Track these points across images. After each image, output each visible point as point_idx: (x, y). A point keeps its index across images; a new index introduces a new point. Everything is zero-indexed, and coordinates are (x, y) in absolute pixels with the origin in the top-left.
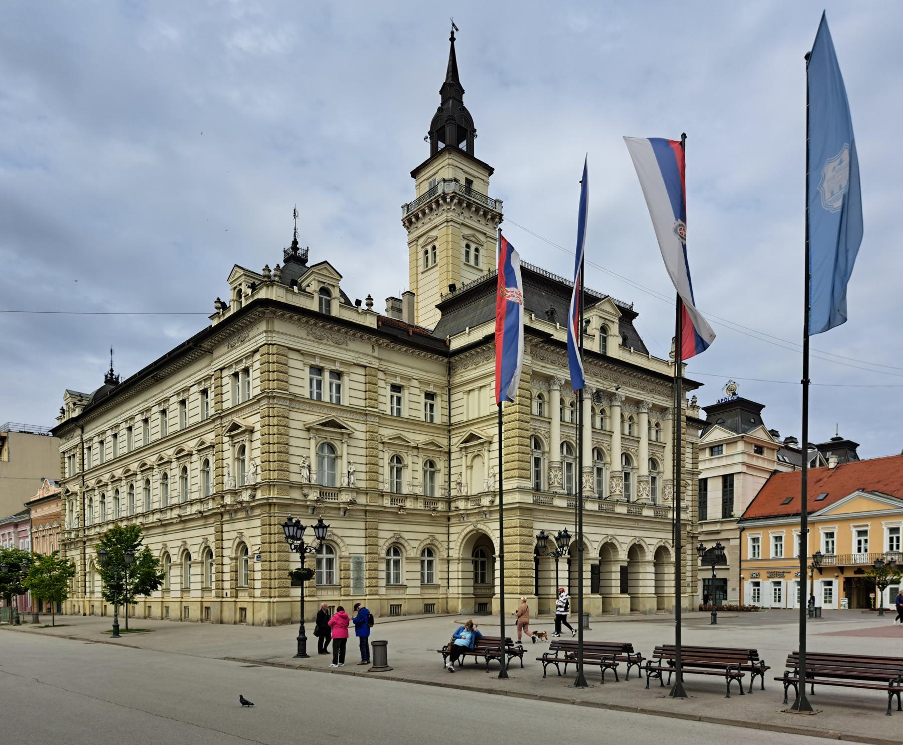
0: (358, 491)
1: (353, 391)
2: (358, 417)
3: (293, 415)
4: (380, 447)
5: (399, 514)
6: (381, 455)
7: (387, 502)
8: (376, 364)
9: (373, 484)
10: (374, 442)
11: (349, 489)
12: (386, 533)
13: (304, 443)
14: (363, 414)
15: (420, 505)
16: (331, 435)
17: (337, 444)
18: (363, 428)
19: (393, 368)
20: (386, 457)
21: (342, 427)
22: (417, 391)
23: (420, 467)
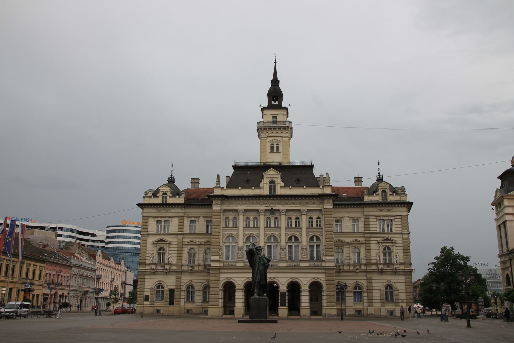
0: (171, 265)
1: (173, 227)
2: (175, 236)
3: (148, 239)
4: (184, 246)
5: (192, 272)
6: (184, 249)
7: (185, 268)
8: (182, 215)
9: (179, 261)
10: (180, 245)
11: (168, 264)
12: (185, 280)
13: (152, 249)
14: (176, 234)
15: (201, 268)
16: (161, 245)
17: (165, 247)
18: (176, 240)
19: (191, 215)
20: (186, 250)
21: (165, 241)
22: (203, 221)
23: (202, 252)
